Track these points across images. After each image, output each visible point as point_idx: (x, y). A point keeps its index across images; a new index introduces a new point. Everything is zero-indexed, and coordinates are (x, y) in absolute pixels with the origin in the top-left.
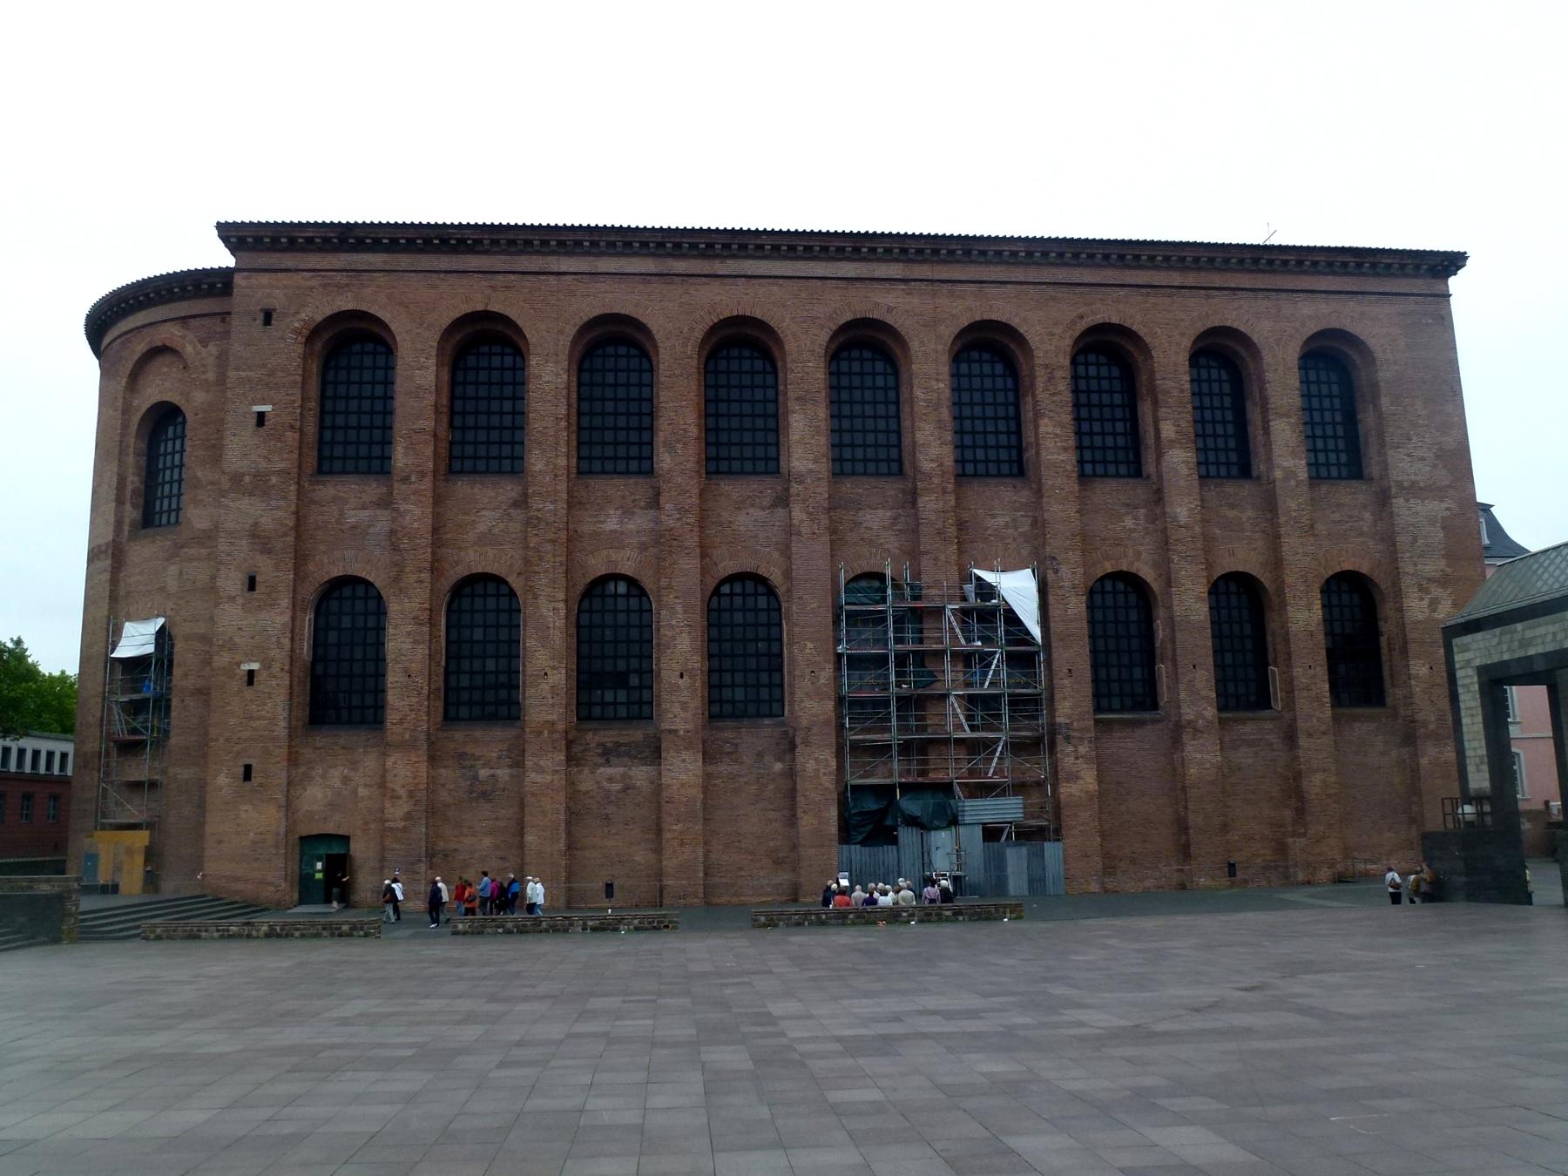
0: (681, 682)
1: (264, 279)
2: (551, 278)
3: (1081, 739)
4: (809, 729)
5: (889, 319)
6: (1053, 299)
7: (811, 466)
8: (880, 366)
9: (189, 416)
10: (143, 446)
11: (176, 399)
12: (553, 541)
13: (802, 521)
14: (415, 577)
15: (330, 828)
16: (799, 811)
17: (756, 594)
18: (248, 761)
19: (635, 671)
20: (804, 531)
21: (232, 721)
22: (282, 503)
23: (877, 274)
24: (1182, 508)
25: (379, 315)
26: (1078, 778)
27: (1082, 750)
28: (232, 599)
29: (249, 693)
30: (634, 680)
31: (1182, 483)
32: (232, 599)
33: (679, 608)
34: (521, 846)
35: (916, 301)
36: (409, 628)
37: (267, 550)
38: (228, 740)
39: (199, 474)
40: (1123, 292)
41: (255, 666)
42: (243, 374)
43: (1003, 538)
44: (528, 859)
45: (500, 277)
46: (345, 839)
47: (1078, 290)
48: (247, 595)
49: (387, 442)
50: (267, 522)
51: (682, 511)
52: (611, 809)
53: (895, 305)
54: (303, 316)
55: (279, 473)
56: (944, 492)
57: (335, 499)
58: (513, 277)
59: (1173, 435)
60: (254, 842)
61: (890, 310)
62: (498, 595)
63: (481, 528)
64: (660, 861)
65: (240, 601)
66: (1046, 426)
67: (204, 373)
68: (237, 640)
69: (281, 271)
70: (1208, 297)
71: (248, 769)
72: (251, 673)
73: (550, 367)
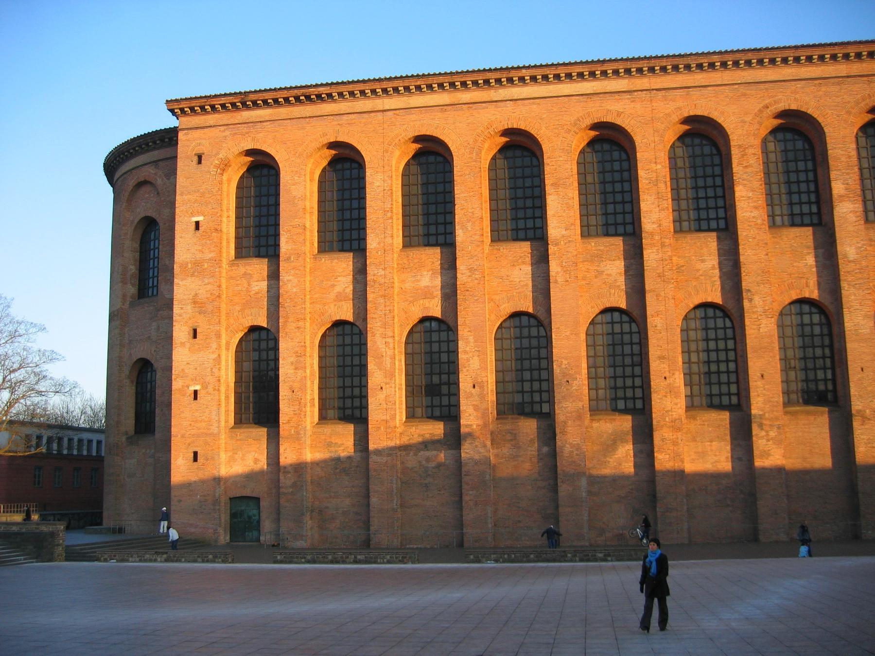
0: (473, 391)
2: (379, 114)
3: (771, 426)
4: (565, 422)
5: (618, 122)
6: (744, 95)
7: (564, 232)
8: (616, 155)
9: (161, 224)
10: (137, 246)
11: (154, 215)
12: (384, 296)
13: (557, 273)
14: (294, 325)
15: (247, 493)
16: (559, 480)
17: (529, 327)
18: (196, 449)
19: (445, 384)
20: (560, 279)
21: (185, 424)
22: (211, 280)
23: (609, 89)
24: (849, 248)
25: (268, 150)
26: (769, 455)
27: (772, 434)
28: (183, 344)
30: (445, 389)
31: (851, 228)
32: (183, 344)
33: (471, 339)
34: (368, 505)
35: (638, 106)
36: (292, 359)
38: (183, 436)
40: (800, 85)
41: (197, 387)
42: (185, 197)
43: (711, 277)
44: (372, 514)
45: (345, 117)
46: (257, 500)
47: (762, 86)
48: (192, 341)
49: (277, 235)
50: (203, 294)
51: (471, 270)
52: (429, 480)
53: (624, 112)
54: (221, 156)
55: (210, 259)
56: (663, 245)
57: (245, 274)
59: (843, 192)
60: (200, 502)
61: (619, 114)
62: (352, 334)
63: (338, 289)
64: (462, 516)
65: (188, 345)
66: (740, 192)
68: (186, 371)
69: (207, 127)
70: (870, 82)
71: (195, 454)
72: (196, 392)
73: (380, 176)
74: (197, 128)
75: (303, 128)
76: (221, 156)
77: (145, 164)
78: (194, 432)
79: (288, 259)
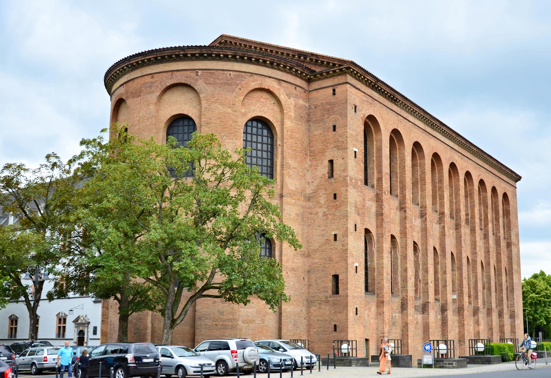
1: (354, 90)
21: (353, 288)
29: (356, 275)
37: (359, 214)
39: (290, 162)
41: (357, 264)
58: (402, 118)
67: (290, 112)
74: (354, 87)
75: (388, 114)
76: (363, 112)
77: (270, 77)
78: (356, 294)
79: (385, 193)
